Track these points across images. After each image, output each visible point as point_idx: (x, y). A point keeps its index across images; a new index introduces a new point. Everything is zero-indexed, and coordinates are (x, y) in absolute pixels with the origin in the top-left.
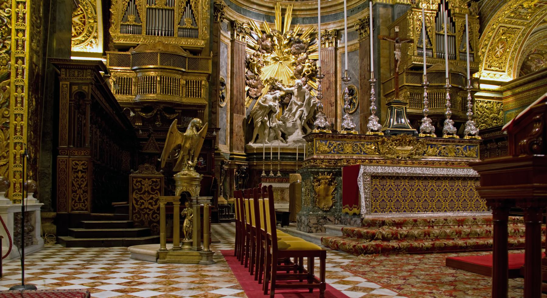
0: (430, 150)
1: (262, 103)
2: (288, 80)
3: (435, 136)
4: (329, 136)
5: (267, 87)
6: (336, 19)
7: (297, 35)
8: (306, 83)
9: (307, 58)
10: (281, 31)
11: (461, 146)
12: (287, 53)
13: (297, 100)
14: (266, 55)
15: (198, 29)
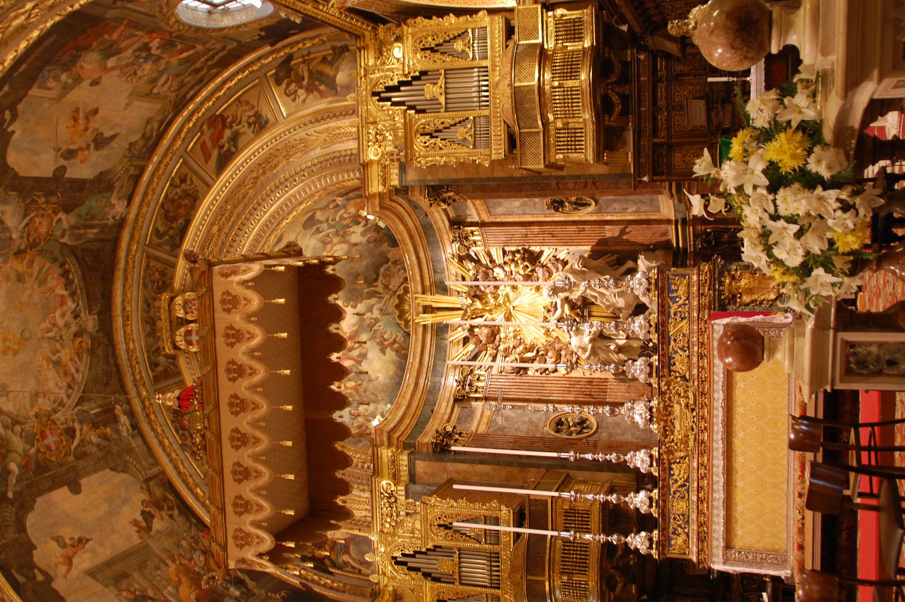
0: (680, 367)
1: (587, 354)
3: (656, 357)
4: (663, 535)
6: (431, 226)
8: (545, 266)
10: (462, 312)
11: (669, 307)
12: (496, 298)
14: (502, 335)
15: (485, 517)
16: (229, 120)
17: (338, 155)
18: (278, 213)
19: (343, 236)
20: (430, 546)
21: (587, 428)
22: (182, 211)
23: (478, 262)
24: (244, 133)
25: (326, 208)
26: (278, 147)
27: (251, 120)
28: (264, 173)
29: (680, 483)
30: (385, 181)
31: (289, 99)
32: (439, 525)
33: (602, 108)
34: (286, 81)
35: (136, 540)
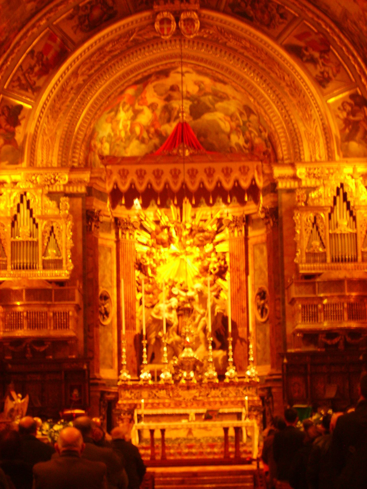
0: (213, 392)
1: (155, 316)
2: (193, 279)
7: (201, 220)
9: (214, 250)
11: (241, 387)
13: (199, 307)
14: (162, 249)
16: (326, 57)
17: (300, 144)
18: (258, 95)
19: (236, 130)
20: (37, 221)
21: (104, 318)
23: (217, 232)
24: (316, 68)
26: (306, 97)
27: (325, 74)
28: (287, 85)
29: (157, 394)
30: (282, 178)
31: (340, 104)
32: (52, 228)
34: (352, 102)
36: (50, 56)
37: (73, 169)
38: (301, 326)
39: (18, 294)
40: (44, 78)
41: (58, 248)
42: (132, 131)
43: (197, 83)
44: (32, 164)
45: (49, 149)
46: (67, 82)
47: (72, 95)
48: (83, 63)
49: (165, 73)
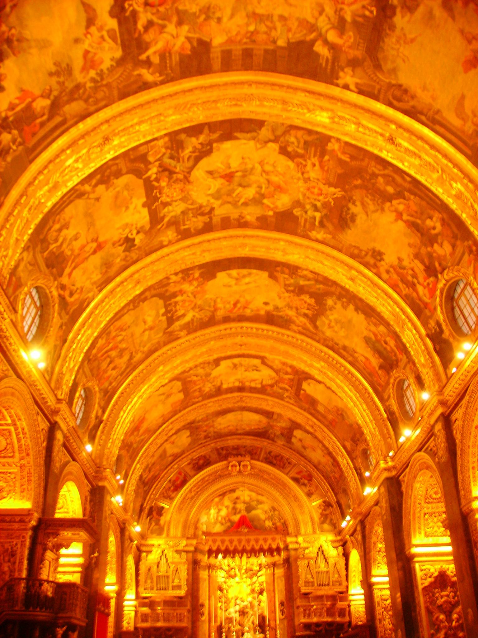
5: (233, 601)
14: (231, 580)
22: (278, 463)
23: (259, 571)
25: (279, 514)
30: (291, 543)
33: (318, 625)
35: (168, 454)
36: (178, 482)
37: (188, 538)
38: (303, 620)
39: (159, 603)
40: (175, 493)
41: (180, 579)
42: (217, 519)
43: (250, 496)
44: (168, 535)
45: (177, 528)
46: (186, 495)
47: (188, 501)
48: (194, 486)
49: (233, 491)
